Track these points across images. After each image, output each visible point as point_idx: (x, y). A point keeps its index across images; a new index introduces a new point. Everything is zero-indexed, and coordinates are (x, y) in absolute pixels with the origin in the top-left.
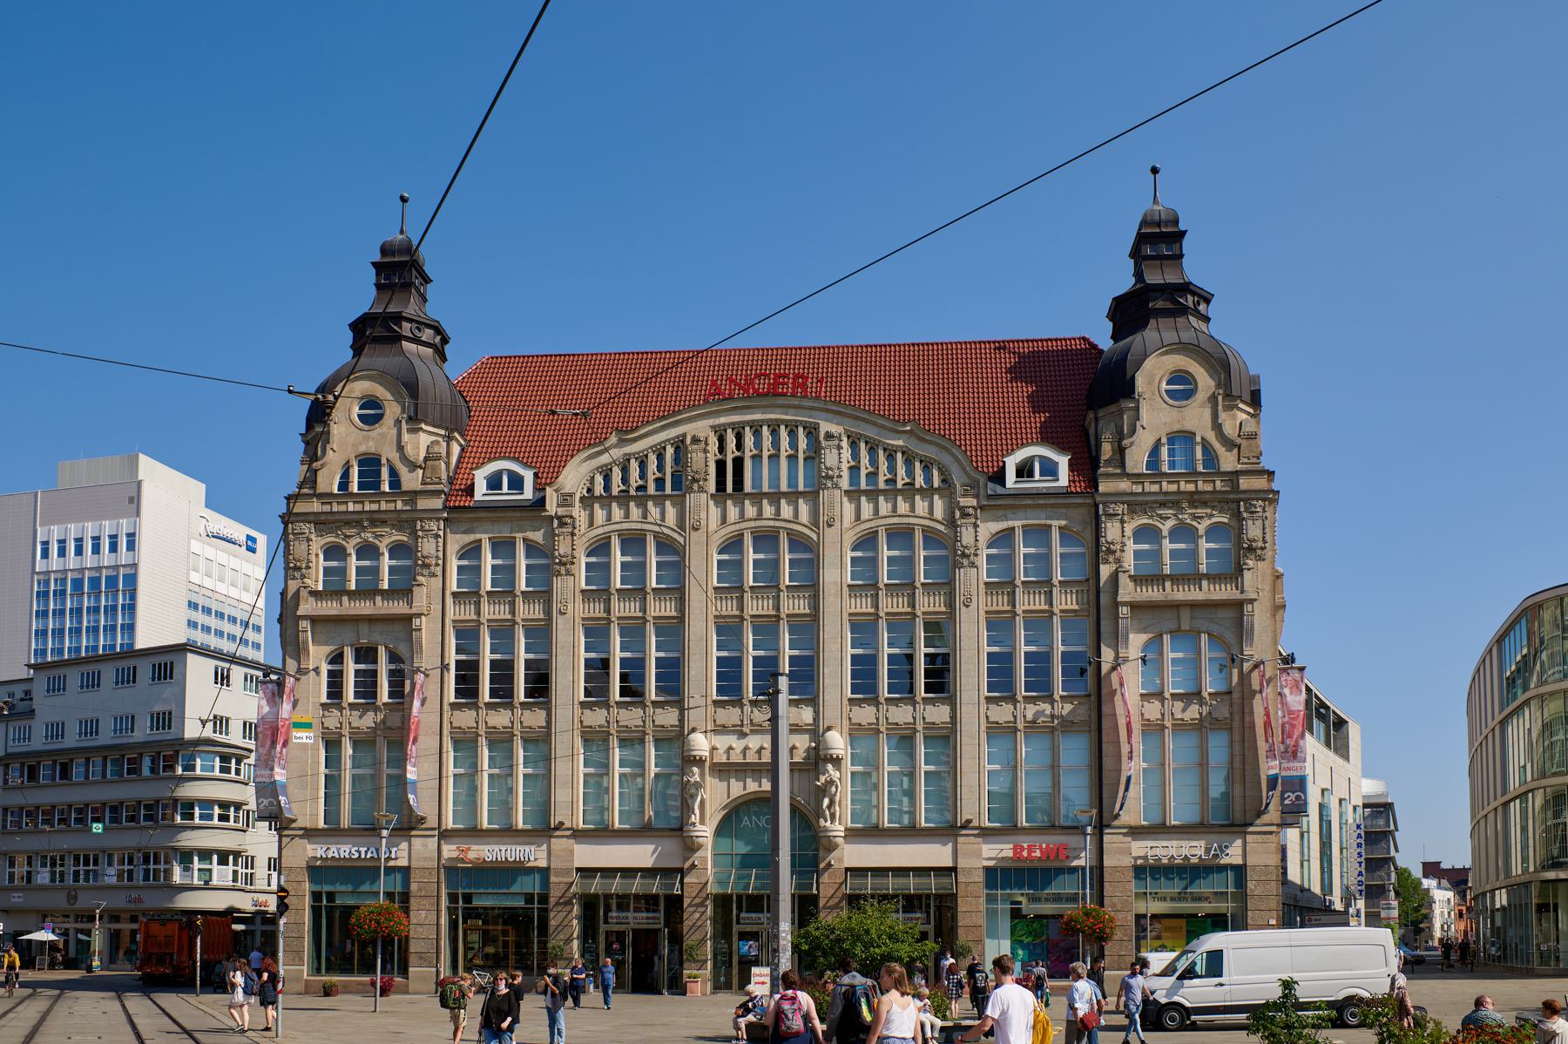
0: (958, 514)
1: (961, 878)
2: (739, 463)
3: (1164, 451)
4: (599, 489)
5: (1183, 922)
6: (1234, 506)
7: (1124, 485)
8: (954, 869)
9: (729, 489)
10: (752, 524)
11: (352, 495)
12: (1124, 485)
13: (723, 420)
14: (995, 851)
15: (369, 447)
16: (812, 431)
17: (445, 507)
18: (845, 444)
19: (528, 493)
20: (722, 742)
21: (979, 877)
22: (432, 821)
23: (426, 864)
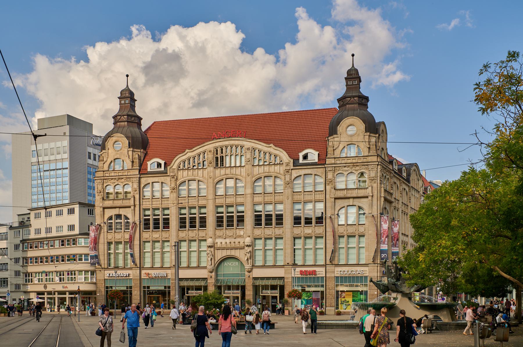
1: (285, 280)
2: (222, 158)
5: (351, 293)
6: (367, 167)
7: (333, 161)
10: (226, 176)
12: (333, 161)
13: (217, 144)
14: (297, 272)
20: (219, 241)
23: (136, 278)
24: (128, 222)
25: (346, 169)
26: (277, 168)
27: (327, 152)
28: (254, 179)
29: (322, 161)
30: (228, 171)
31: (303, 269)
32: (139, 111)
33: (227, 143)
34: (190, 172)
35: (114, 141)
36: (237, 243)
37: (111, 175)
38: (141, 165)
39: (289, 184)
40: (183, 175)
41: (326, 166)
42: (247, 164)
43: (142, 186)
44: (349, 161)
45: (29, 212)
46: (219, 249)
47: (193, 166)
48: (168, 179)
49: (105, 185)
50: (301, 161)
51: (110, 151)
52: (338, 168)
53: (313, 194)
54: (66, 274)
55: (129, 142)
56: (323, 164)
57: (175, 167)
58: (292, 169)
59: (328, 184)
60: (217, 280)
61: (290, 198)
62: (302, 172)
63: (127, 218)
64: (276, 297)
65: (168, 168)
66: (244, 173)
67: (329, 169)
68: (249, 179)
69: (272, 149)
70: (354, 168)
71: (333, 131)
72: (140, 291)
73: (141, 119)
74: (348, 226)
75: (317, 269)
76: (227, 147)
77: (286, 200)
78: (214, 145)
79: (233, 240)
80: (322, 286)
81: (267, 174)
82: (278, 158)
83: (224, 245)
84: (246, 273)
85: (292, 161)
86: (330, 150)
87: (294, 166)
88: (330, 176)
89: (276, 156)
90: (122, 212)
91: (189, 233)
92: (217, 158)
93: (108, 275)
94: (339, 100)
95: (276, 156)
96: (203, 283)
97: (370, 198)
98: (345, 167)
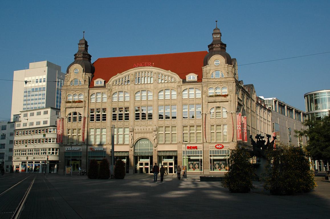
4: (115, 84)
6: (227, 84)
8: (177, 151)
10: (141, 89)
12: (206, 80)
13: (137, 70)
24: (80, 117)
25: (214, 85)
26: (173, 84)
27: (202, 75)
28: (158, 91)
29: (200, 80)
30: (143, 86)
32: (90, 52)
33: (142, 70)
34: (120, 87)
35: (74, 69)
38: (89, 83)
39: (180, 94)
40: (116, 89)
41: (202, 83)
43: (90, 95)
44: (216, 80)
47: (122, 83)
48: (106, 90)
49: (67, 94)
51: (71, 74)
52: (209, 85)
53: (195, 100)
54: (34, 150)
55: (83, 69)
58: (182, 85)
60: (134, 152)
61: (181, 103)
63: (80, 114)
64: (172, 163)
65: (107, 84)
66: (152, 88)
67: (204, 85)
69: (169, 73)
72: (87, 159)
73: (91, 56)
77: (179, 103)
78: (135, 71)
79: (145, 128)
80: (201, 156)
83: (140, 131)
84: (154, 148)
85: (182, 80)
88: (205, 89)
91: (118, 123)
93: (66, 149)
94: (209, 46)
95: (172, 78)
97: (229, 102)
98: (214, 84)
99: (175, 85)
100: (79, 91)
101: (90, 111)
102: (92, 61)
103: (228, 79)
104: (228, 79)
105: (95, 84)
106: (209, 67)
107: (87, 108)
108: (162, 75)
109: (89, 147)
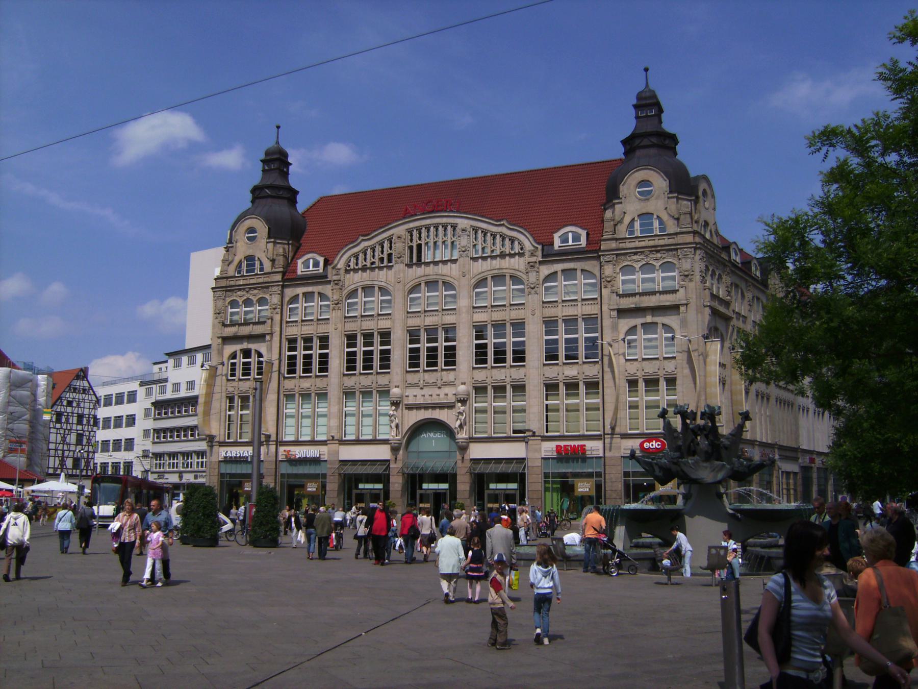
0: (528, 266)
2: (419, 246)
3: (637, 225)
7: (613, 245)
9: (415, 261)
11: (243, 276)
12: (613, 245)
13: (412, 225)
14: (548, 449)
15: (250, 252)
16: (454, 227)
17: (283, 280)
18: (472, 233)
19: (321, 269)
20: (410, 392)
21: (538, 463)
22: (273, 438)
25: (635, 257)
30: (430, 270)
31: (562, 443)
33: (428, 222)
36: (442, 396)
37: (238, 283)
40: (356, 279)
42: (461, 256)
43: (286, 299)
45: (166, 358)
46: (410, 407)
50: (557, 243)
51: (238, 244)
56: (597, 251)
57: (341, 265)
58: (540, 262)
59: (606, 287)
62: (558, 267)
67: (607, 258)
68: (464, 281)
70: (652, 256)
71: (612, 195)
74: (645, 363)
75: (589, 444)
76: (428, 228)
79: (438, 391)
81: (496, 271)
82: (516, 243)
83: (420, 400)
85: (540, 247)
86: (608, 226)
87: (543, 256)
89: (512, 240)
90: (253, 346)
91: (360, 380)
92: (411, 248)
94: (625, 142)
95: (512, 240)
96: (379, 470)
99: (518, 264)
100: (256, 291)
101: (285, 345)
102: (303, 204)
103: (680, 239)
104: (680, 239)
105: (300, 269)
106: (621, 203)
107: (276, 338)
108: (485, 233)
109: (282, 449)
